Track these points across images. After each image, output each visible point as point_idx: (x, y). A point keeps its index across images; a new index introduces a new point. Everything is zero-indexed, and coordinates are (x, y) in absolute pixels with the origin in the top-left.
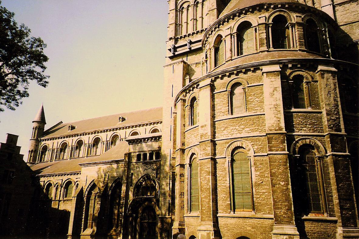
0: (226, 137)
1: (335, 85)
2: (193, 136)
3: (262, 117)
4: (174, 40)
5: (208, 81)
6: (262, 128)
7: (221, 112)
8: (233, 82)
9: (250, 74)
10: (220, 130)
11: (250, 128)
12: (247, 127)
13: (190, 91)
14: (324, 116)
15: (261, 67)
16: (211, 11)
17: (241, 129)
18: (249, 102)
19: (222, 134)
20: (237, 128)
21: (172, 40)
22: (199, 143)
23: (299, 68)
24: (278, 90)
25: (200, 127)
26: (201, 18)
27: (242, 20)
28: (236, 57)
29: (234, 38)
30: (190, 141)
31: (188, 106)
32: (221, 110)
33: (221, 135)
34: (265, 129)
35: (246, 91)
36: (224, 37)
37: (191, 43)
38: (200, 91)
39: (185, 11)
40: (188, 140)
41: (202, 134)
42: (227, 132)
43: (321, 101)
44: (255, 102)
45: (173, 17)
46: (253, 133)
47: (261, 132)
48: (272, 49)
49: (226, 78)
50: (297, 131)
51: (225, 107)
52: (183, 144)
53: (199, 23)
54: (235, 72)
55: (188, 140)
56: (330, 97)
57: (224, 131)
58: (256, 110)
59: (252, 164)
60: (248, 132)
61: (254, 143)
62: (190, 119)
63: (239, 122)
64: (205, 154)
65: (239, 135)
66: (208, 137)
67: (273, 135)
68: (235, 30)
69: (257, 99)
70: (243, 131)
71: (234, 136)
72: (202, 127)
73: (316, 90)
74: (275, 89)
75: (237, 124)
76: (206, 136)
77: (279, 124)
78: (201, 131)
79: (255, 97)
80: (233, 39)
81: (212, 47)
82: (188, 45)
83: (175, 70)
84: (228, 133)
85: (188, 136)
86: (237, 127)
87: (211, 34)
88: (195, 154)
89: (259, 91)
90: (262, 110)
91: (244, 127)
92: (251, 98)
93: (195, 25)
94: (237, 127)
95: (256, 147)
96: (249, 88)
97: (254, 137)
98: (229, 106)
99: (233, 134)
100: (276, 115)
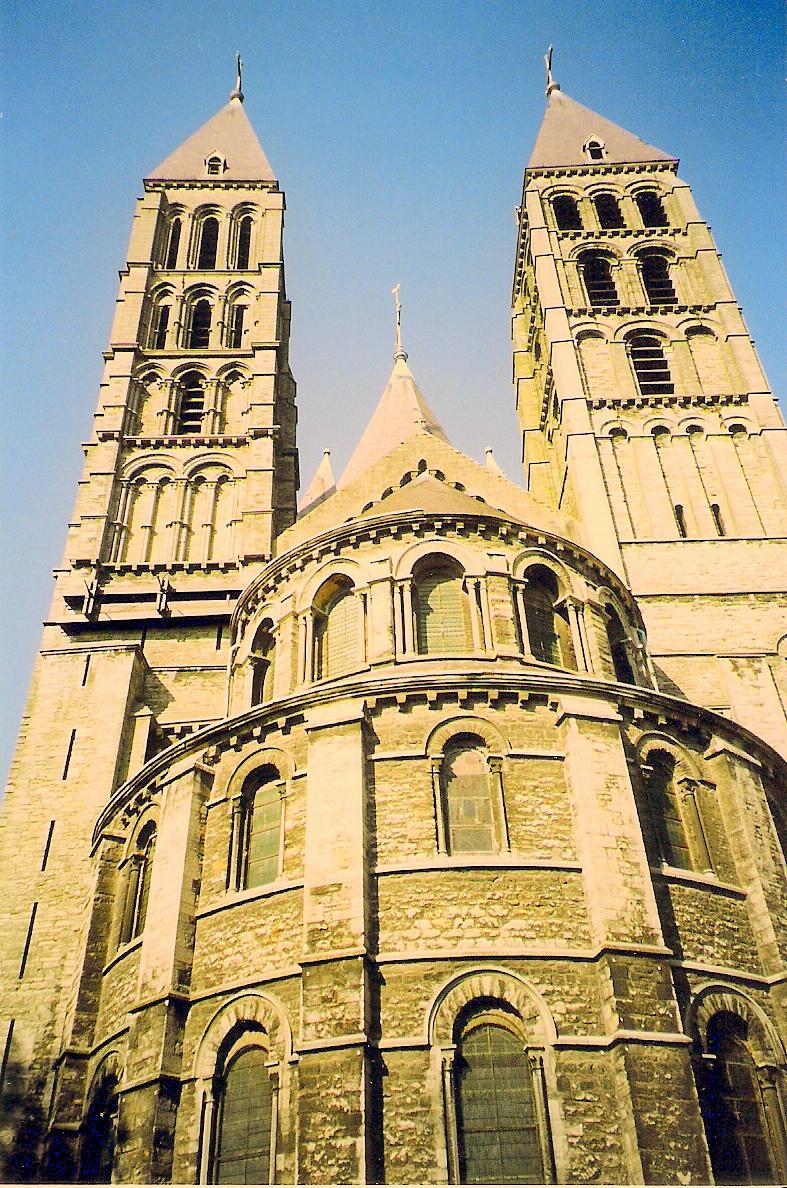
1: (764, 809)
2: (247, 936)
3: (571, 881)
4: (94, 571)
5: (353, 708)
6: (575, 925)
7: (404, 836)
8: (452, 729)
9: (513, 710)
10: (399, 915)
12: (517, 915)
13: (248, 738)
14: (759, 912)
15: (552, 697)
16: (252, 517)
17: (494, 920)
18: (520, 813)
19: (412, 933)
20: (476, 911)
21: (84, 570)
22: (299, 970)
23: (661, 727)
24: (622, 788)
25: (306, 891)
26: (209, 527)
29: (401, 593)
30: (226, 963)
31: (226, 800)
32: (403, 831)
33: (405, 938)
34: (585, 933)
35: (505, 768)
37: (174, 595)
38: (312, 740)
39: (147, 493)
40: (214, 957)
41: (319, 927)
42: (434, 926)
43: (735, 857)
44: (541, 816)
45: (100, 496)
47: (572, 944)
49: (420, 711)
50: (689, 954)
51: (422, 819)
52: (184, 976)
53: (201, 536)
54: (463, 694)
55: (214, 957)
56: (763, 845)
57: (417, 923)
58: (546, 847)
59: (552, 1083)
61: (550, 988)
62: (234, 860)
63: (483, 890)
64: (334, 1022)
65: (485, 947)
66: (350, 941)
67: (628, 959)
68: (405, 571)
69: (546, 808)
70: (503, 930)
72: (319, 892)
73: (715, 812)
74: (612, 782)
75: (474, 897)
76: (340, 935)
77: (640, 914)
78: (314, 912)
79: (541, 800)
80: (397, 596)
82: (159, 597)
83: (93, 676)
84: (438, 932)
85: (219, 935)
86: (477, 907)
87: (302, 569)
89: (551, 779)
90: (569, 851)
91: (505, 912)
92: (526, 799)
93: (182, 545)
94: (477, 907)
95: (561, 1007)
96: (514, 761)
97: (550, 962)
98: (435, 817)
100: (629, 880)
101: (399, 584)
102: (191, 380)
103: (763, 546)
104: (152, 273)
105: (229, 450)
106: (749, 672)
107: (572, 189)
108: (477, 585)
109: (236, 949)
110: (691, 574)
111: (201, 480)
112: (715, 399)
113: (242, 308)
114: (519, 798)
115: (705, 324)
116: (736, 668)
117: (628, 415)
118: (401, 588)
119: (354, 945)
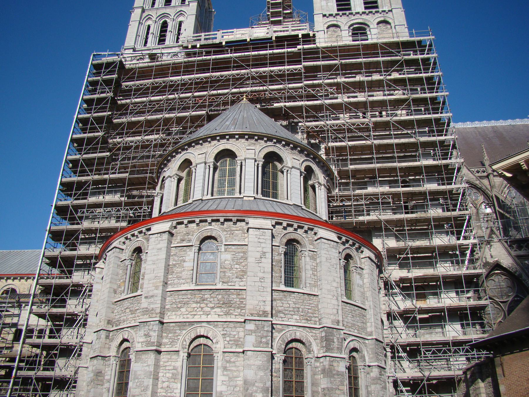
0: (184, 318)
11: (222, 309)
19: (179, 313)
22: (138, 324)
25: (143, 297)
28: (209, 197)
36: (194, 164)
46: (225, 317)
47: (237, 317)
48: (260, 196)
60: (219, 315)
64: (147, 342)
65: (204, 318)
71: (197, 319)
80: (207, 170)
81: (174, 175)
84: (187, 313)
88: (129, 342)
99: (195, 315)
101: (208, 164)
104: (143, 11)
109: (125, 314)
118: (209, 166)
119: (156, 317)
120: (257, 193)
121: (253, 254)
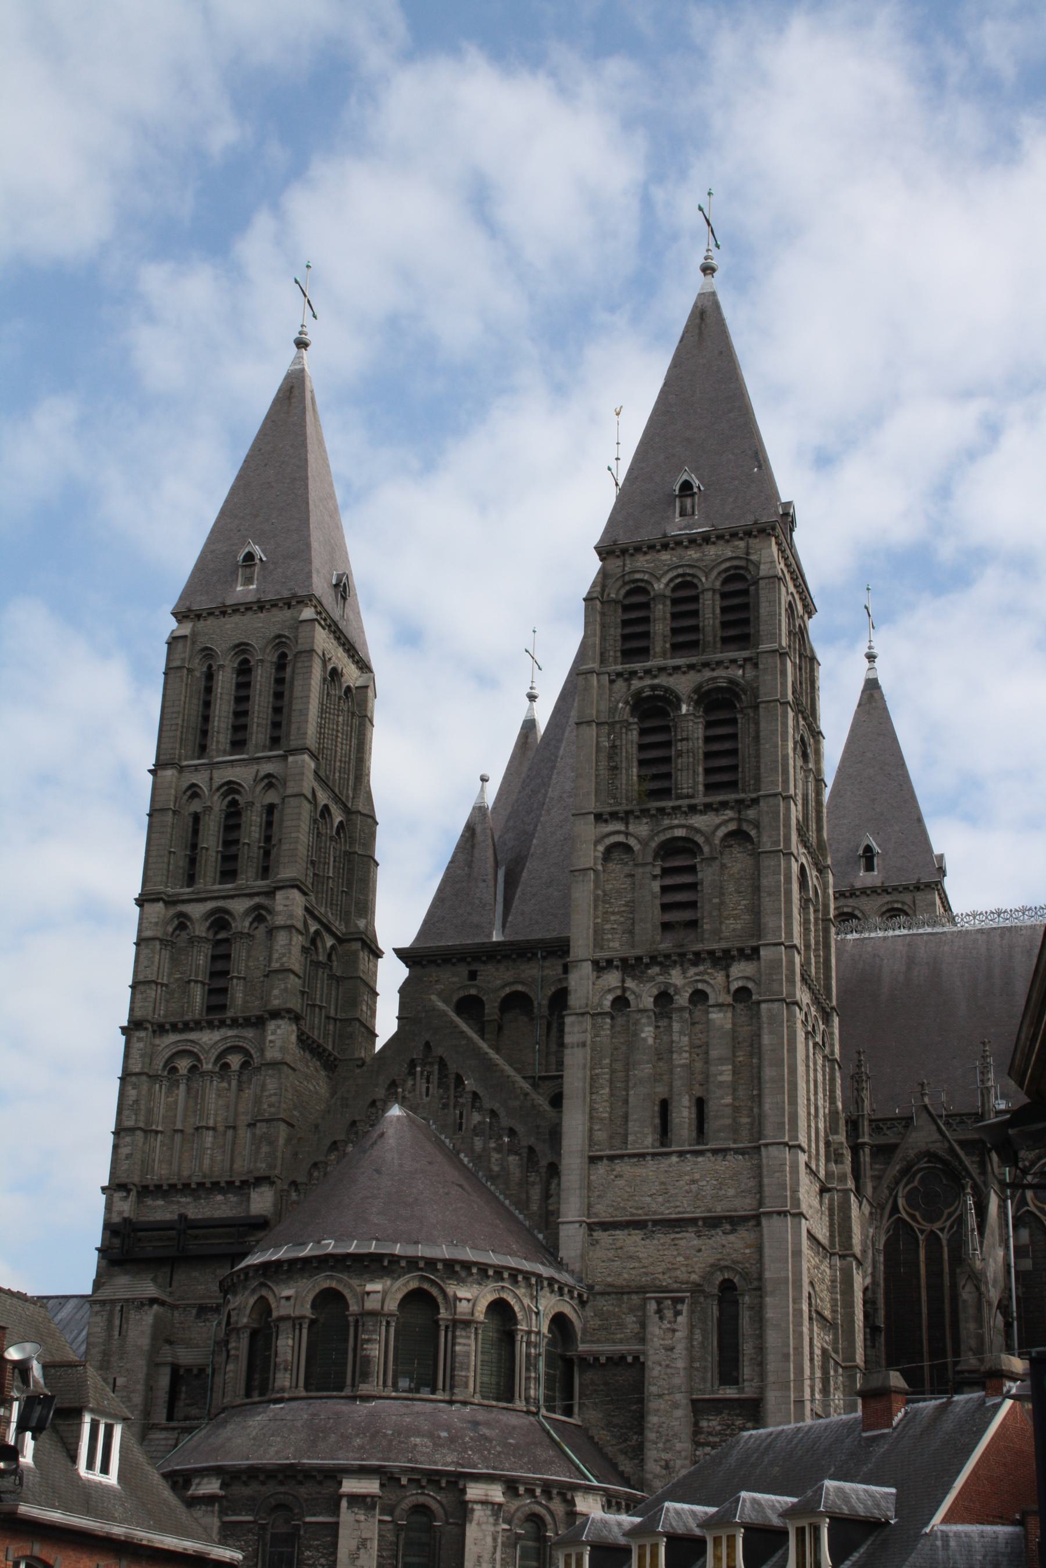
1: (495, 1539)
27: (327, 1284)
74: (363, 1543)
80: (297, 1331)
102: (220, 921)
103: (728, 1157)
105: (249, 1033)
106: (669, 1314)
107: (646, 577)
108: (357, 1321)
110: (650, 1196)
111: (226, 1066)
112: (726, 952)
113: (271, 809)
114: (308, 1553)
115: (745, 827)
116: (659, 1311)
117: (634, 978)
120: (385, 1385)
121: (346, 1544)
